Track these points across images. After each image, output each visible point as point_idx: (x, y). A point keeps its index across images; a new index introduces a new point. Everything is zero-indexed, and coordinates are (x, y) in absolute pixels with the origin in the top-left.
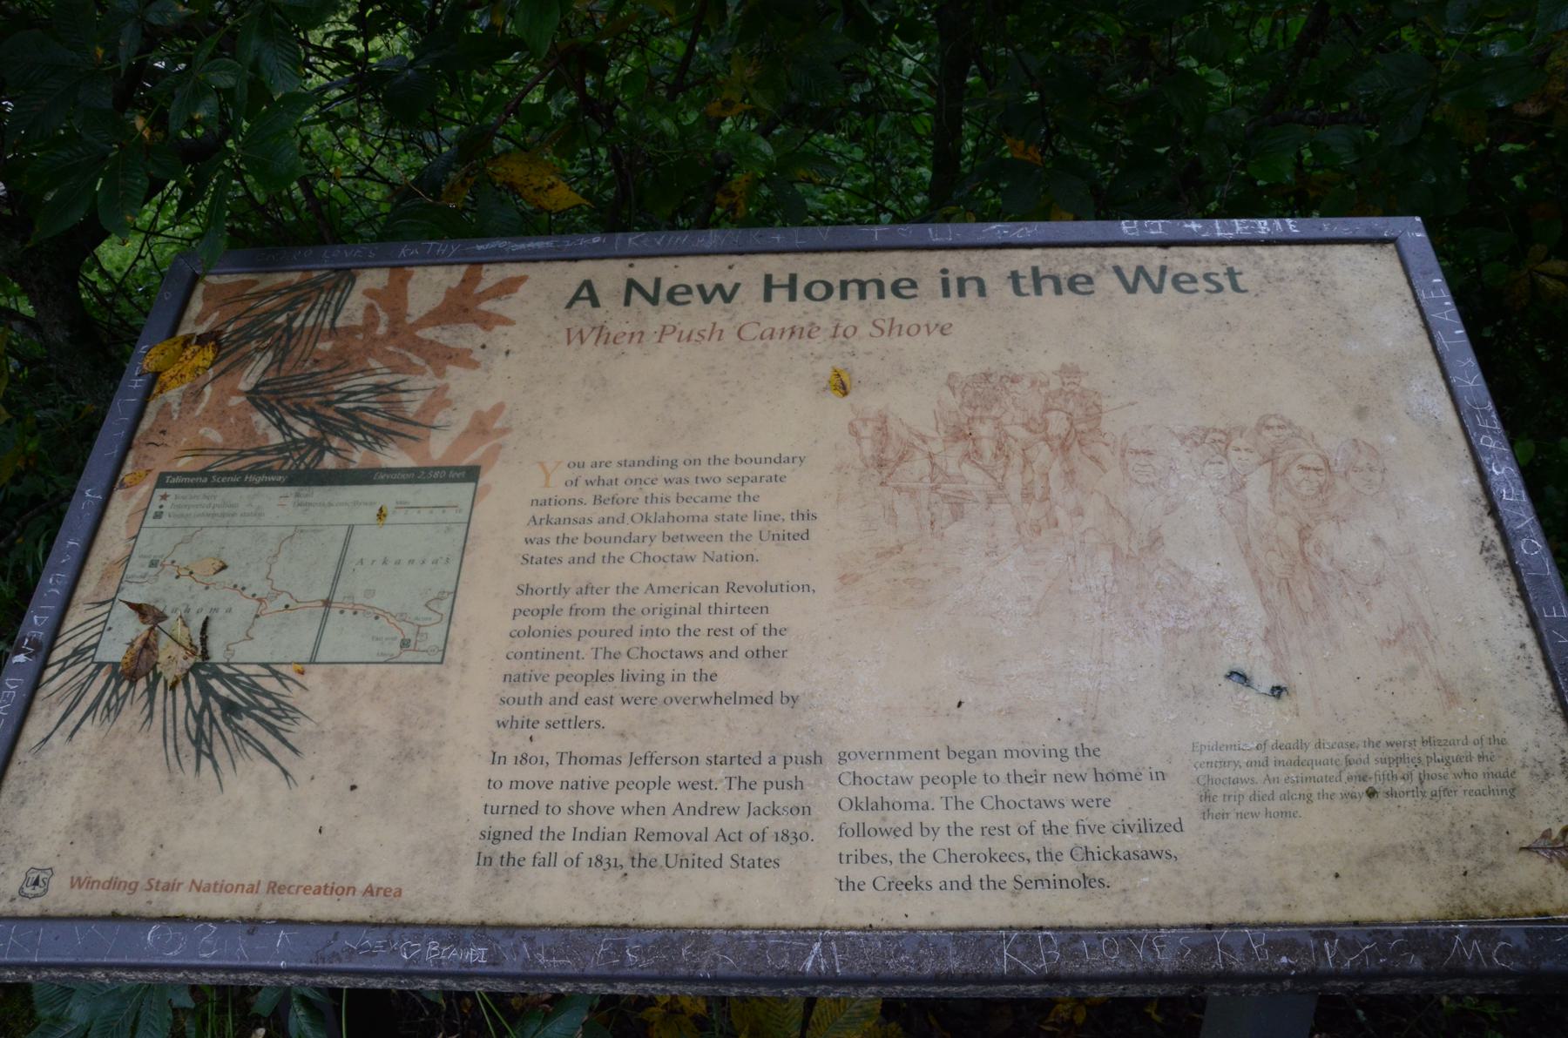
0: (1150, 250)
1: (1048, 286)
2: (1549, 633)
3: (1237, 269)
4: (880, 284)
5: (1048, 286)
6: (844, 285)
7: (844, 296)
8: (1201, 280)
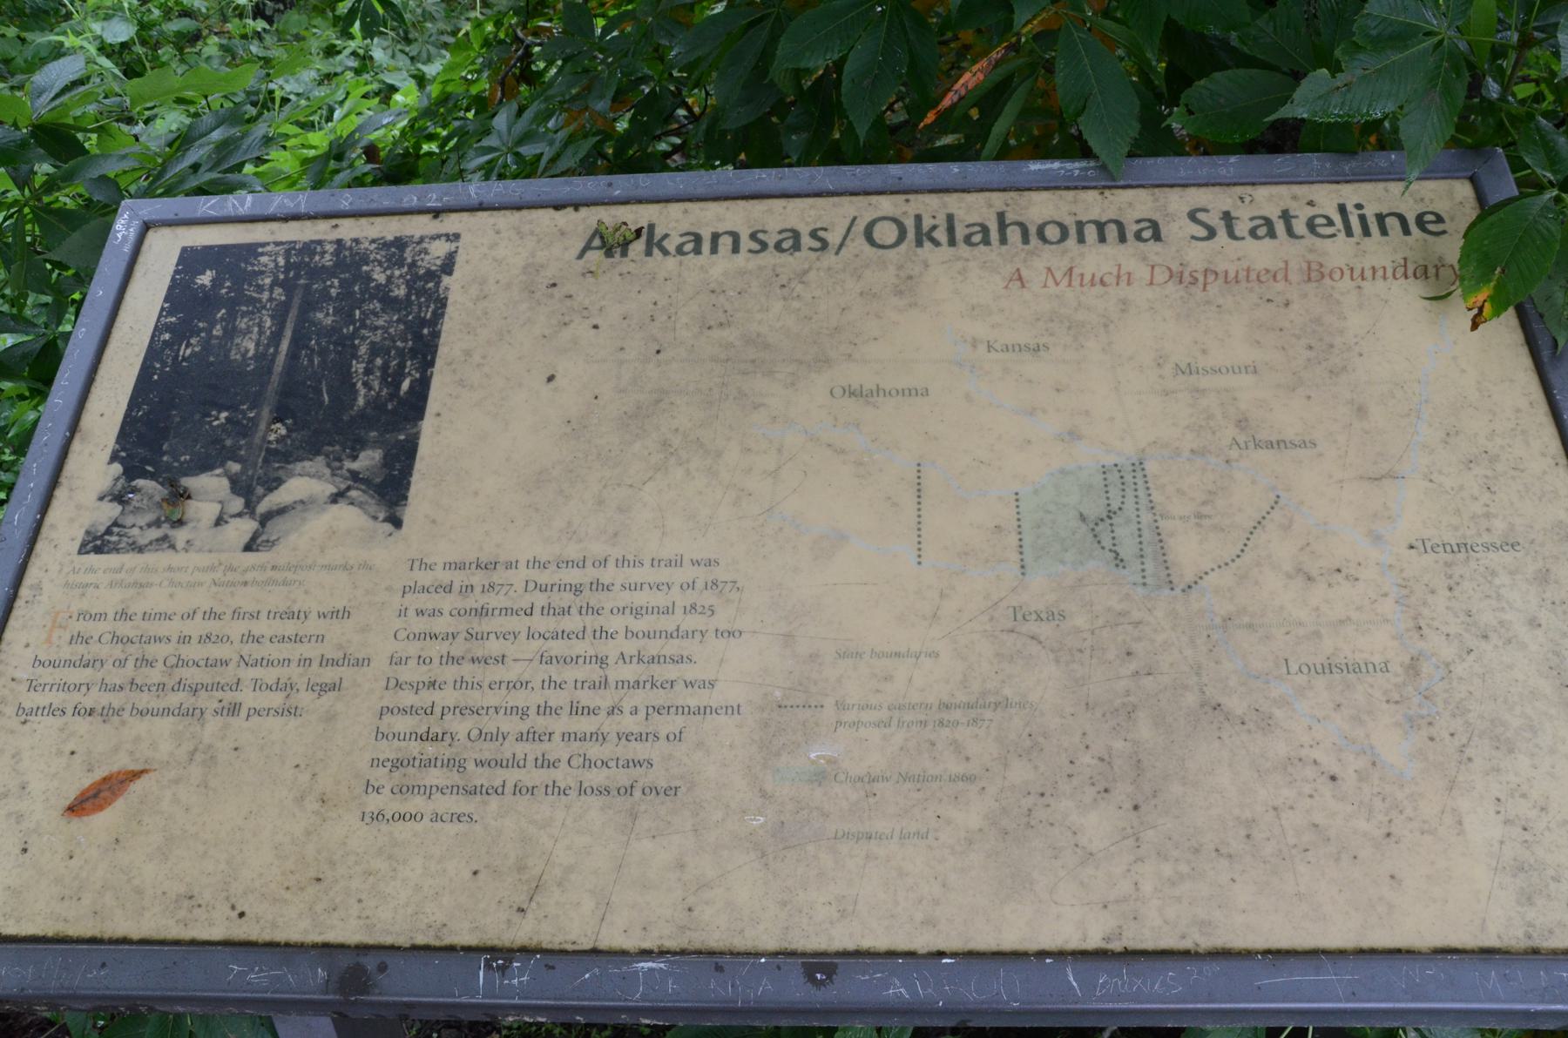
0: (541, 212)
1: (1014, 234)
2: (1100, 1000)
3: (1292, 213)
4: (735, 237)
5: (1014, 234)
6: (715, 237)
7: (714, 250)
8: (771, 243)
